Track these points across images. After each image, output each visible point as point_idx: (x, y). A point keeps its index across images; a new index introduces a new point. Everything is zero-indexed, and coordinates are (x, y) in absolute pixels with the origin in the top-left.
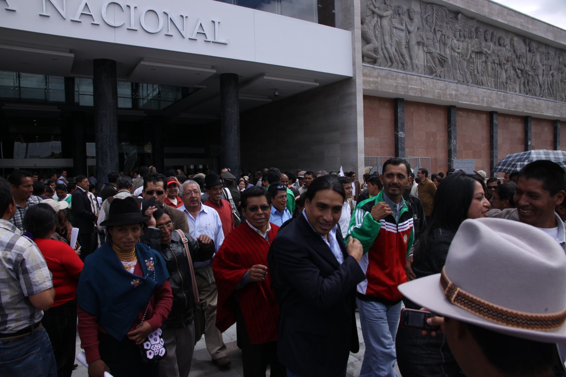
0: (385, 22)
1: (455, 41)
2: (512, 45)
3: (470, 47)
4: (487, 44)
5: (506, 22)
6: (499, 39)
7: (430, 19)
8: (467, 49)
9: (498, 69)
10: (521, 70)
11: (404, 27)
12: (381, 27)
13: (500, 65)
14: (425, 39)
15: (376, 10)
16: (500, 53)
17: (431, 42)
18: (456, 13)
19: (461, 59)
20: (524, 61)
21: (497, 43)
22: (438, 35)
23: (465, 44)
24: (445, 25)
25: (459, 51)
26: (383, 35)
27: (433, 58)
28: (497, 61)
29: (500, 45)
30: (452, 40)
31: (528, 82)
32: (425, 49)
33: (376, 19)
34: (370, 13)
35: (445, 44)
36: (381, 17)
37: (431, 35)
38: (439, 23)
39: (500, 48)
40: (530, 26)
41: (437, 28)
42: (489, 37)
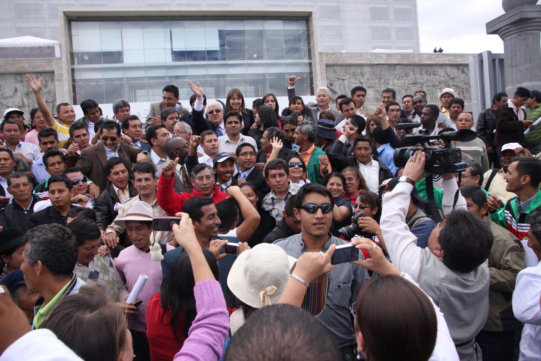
0: (346, 82)
1: (396, 81)
2: (446, 73)
3: (406, 82)
4: (423, 76)
5: (435, 62)
6: (434, 71)
7: (376, 73)
8: (405, 83)
9: (434, 89)
10: (456, 86)
11: (358, 82)
12: (344, 85)
13: (434, 86)
14: (373, 84)
15: (341, 77)
16: (434, 80)
17: (378, 85)
18: (396, 65)
19: (401, 89)
20: (457, 80)
21: (432, 74)
22: (383, 81)
23: (403, 81)
24: (387, 73)
25: (399, 85)
26: (345, 88)
27: (379, 93)
28: (431, 85)
29: (435, 75)
30: (393, 80)
31: (463, 92)
32: (374, 89)
33: (340, 81)
34: (336, 79)
35: (388, 84)
36: (343, 80)
37: (377, 81)
38: (383, 73)
39: (434, 76)
40: (459, 60)
41: (381, 77)
42: (423, 73)
